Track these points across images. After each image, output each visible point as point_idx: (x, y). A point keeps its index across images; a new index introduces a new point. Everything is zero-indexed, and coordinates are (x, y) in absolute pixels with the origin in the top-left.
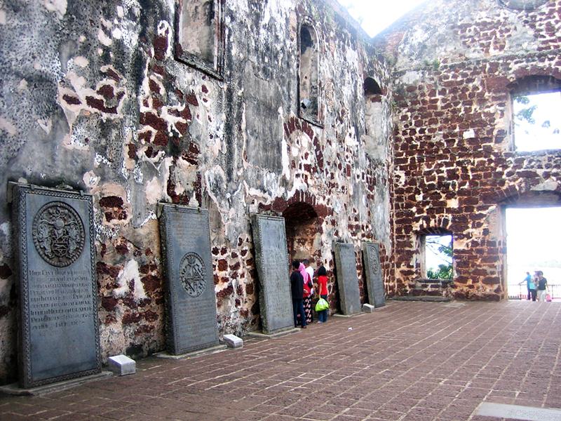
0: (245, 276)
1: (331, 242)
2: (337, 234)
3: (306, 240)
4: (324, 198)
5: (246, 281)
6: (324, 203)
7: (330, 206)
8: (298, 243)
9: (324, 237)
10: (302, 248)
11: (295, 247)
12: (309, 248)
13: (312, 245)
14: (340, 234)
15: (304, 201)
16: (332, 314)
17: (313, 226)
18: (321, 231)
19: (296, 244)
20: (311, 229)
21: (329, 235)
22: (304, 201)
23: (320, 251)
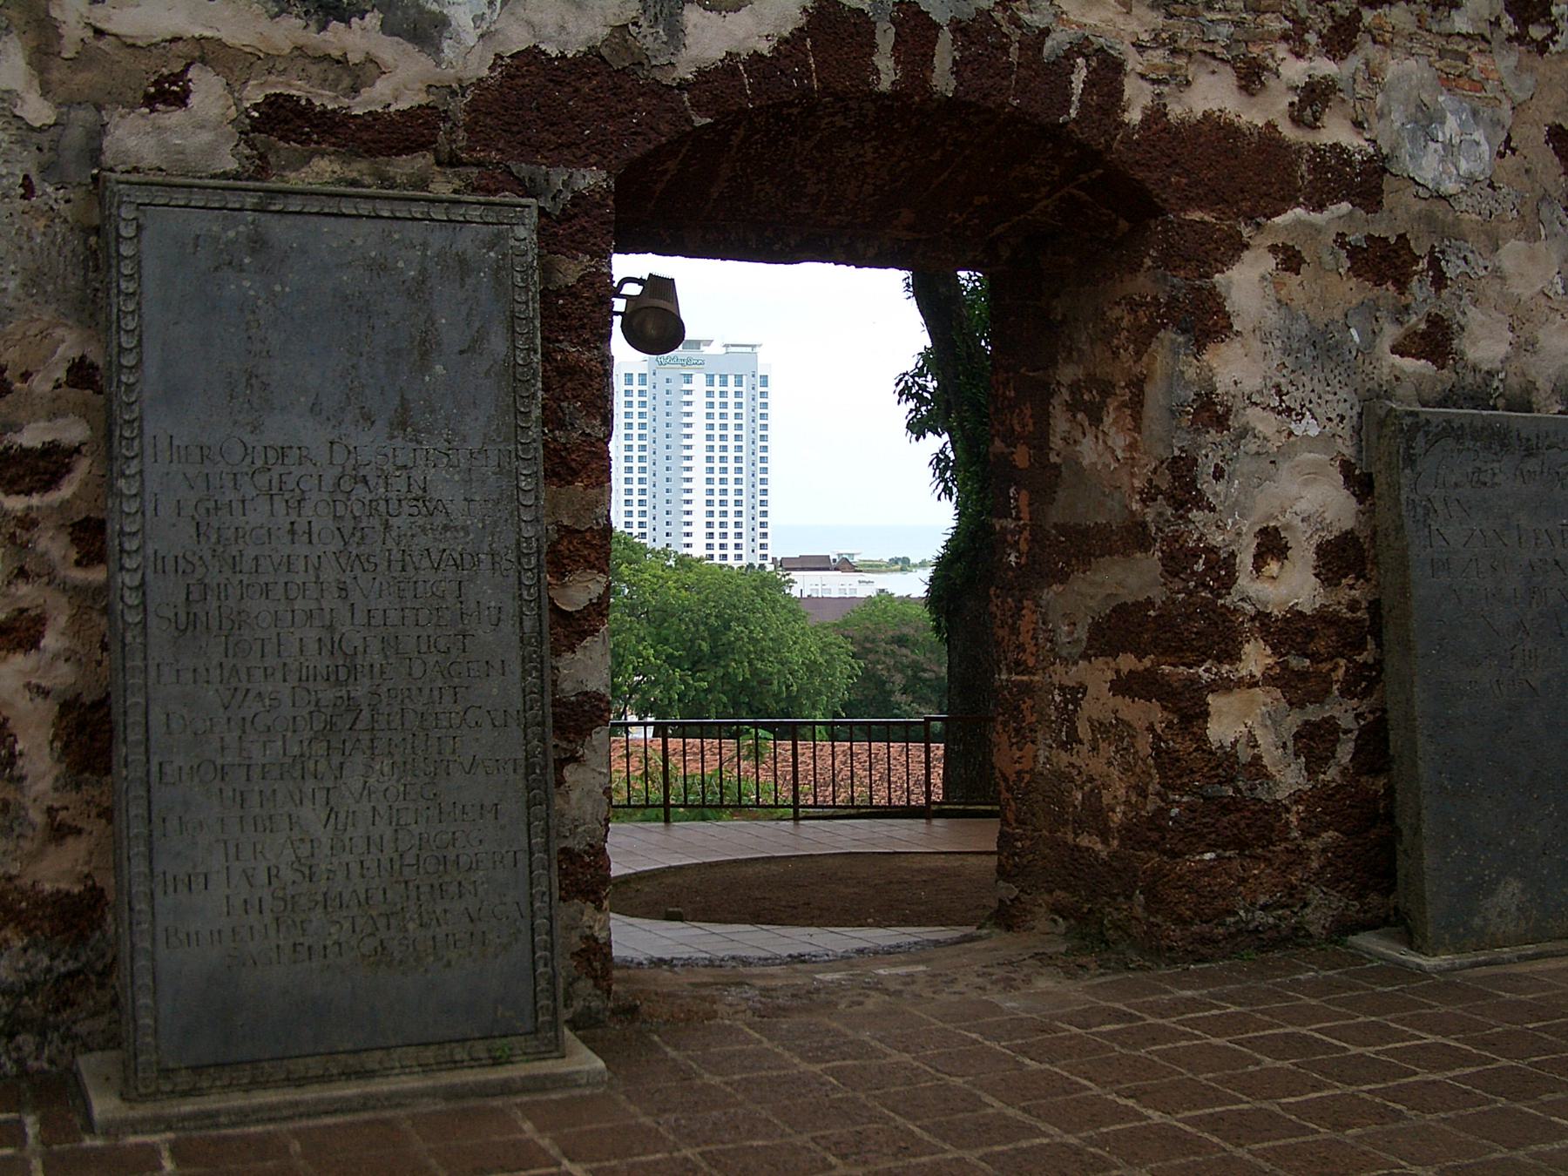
0: (50, 641)
1: (1342, 402)
2: (1435, 341)
3: (1107, 389)
4: (1251, 77)
5: (63, 676)
6: (1266, 111)
7: (1336, 131)
8: (1072, 408)
9: (1235, 368)
10: (1089, 451)
11: (1056, 442)
12: (1119, 441)
13: (1137, 417)
14: (1485, 345)
15: (943, 80)
16: (1344, 928)
17: (1142, 284)
18: (1207, 322)
19: (1060, 424)
20: (1133, 305)
21: (1321, 346)
22: (943, 80)
23: (1182, 469)
